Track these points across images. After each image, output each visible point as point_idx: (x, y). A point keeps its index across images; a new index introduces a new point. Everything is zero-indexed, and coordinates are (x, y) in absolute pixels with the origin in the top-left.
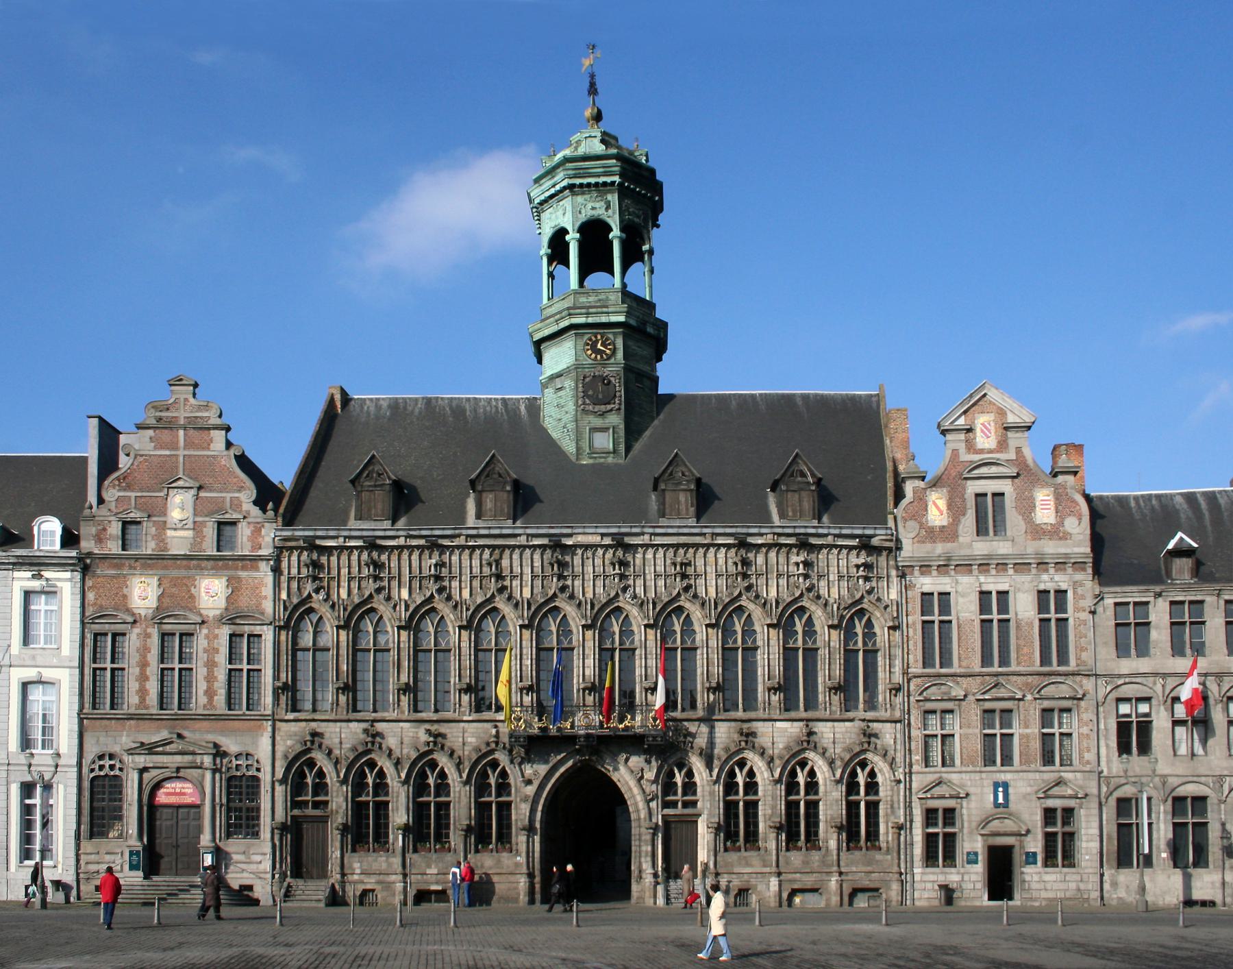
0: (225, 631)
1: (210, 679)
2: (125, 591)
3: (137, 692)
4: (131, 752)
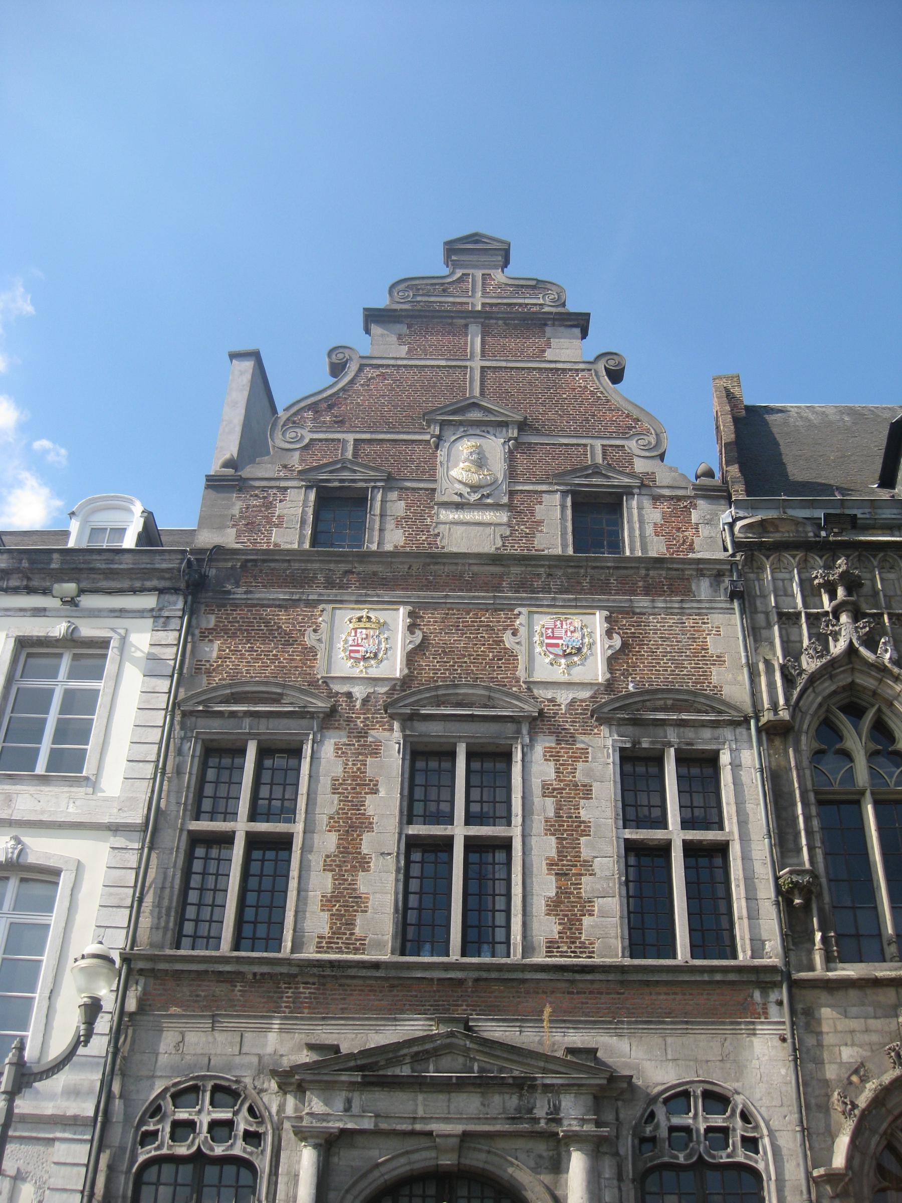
0: (602, 750)
1: (569, 866)
2: (310, 639)
3: (328, 902)
4: (294, 1081)
